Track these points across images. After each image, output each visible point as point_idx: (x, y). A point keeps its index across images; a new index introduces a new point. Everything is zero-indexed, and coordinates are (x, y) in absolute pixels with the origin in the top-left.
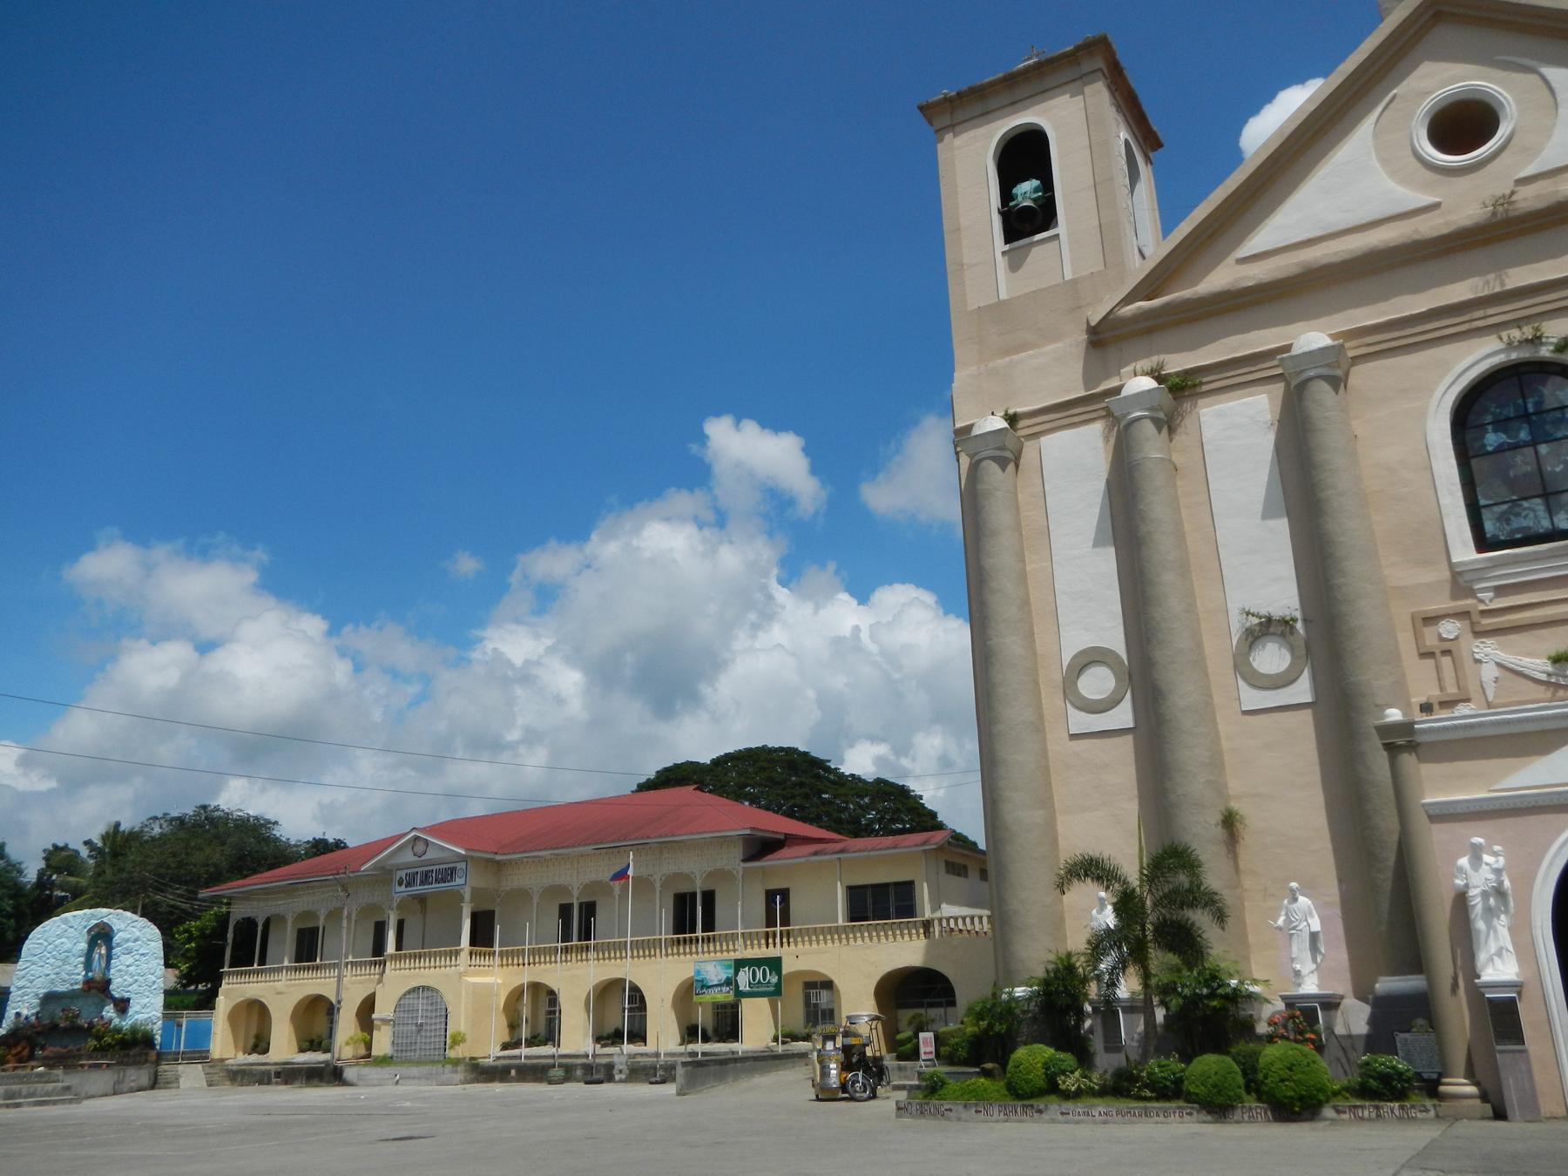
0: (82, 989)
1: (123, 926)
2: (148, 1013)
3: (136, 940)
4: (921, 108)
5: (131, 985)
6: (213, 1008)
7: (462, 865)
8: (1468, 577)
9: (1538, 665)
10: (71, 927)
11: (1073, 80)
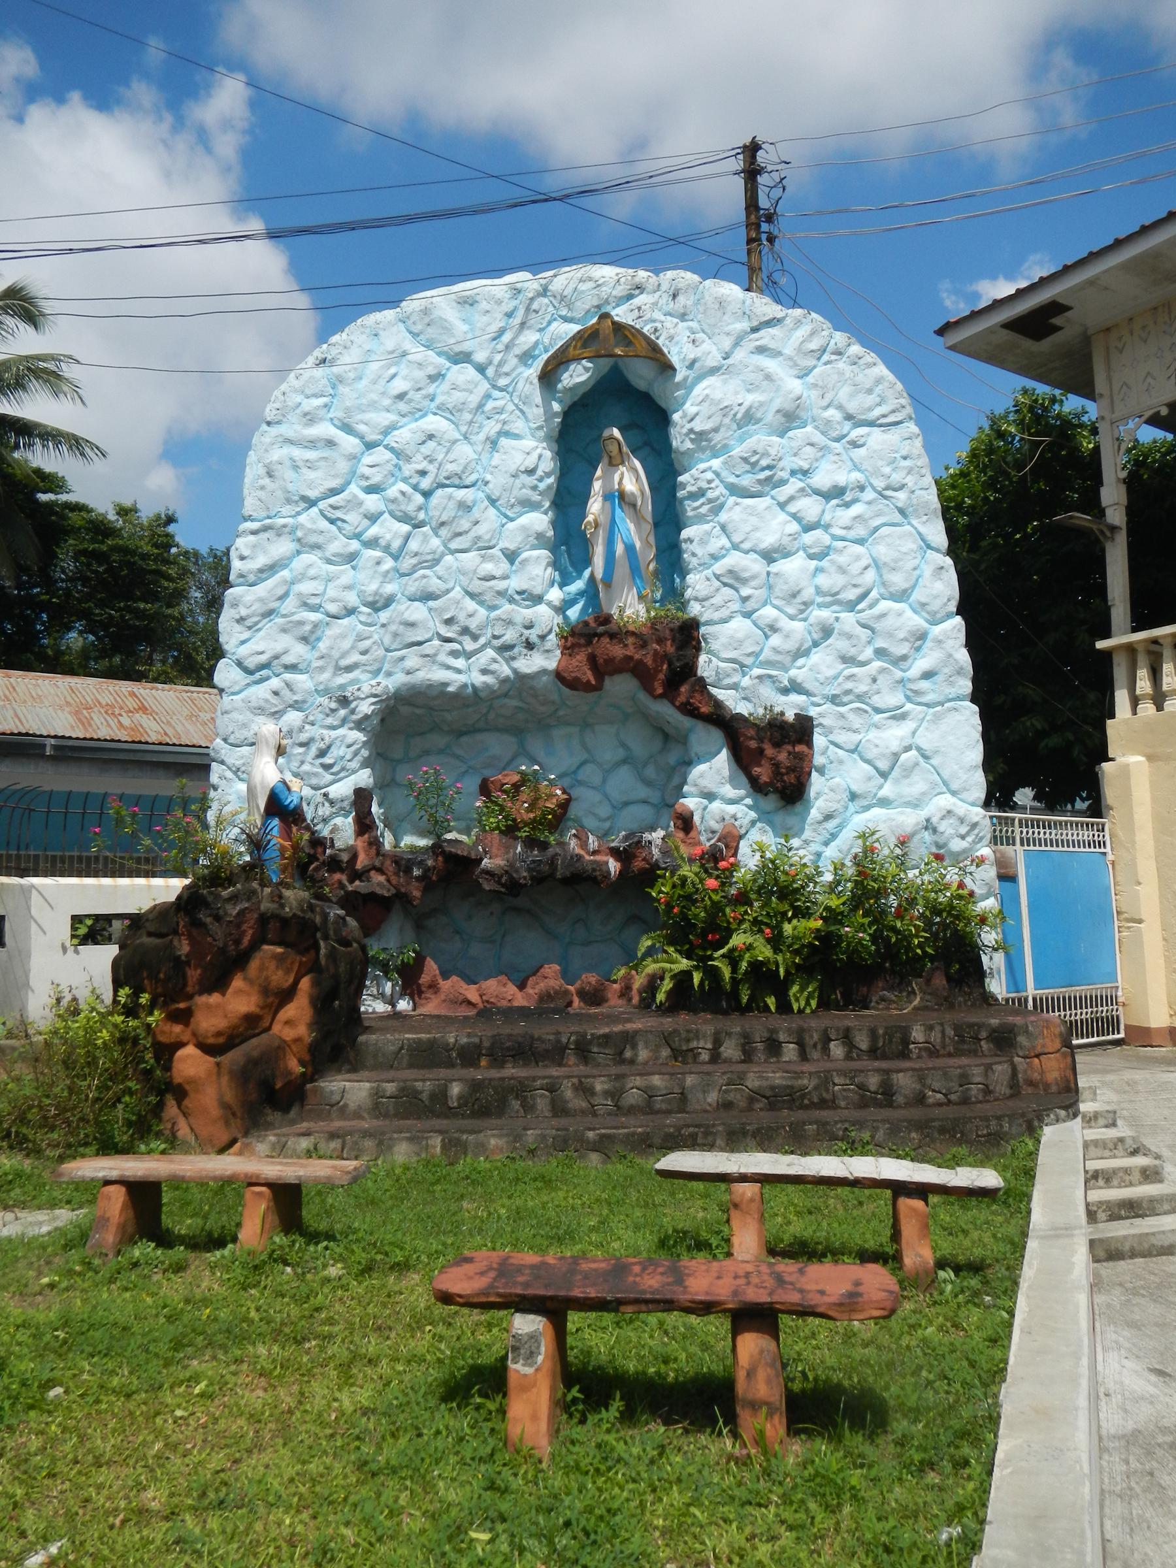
0: (558, 675)
1: (710, 351)
2: (915, 804)
3: (790, 418)
5: (801, 653)
6: (1097, 810)
10: (462, 358)
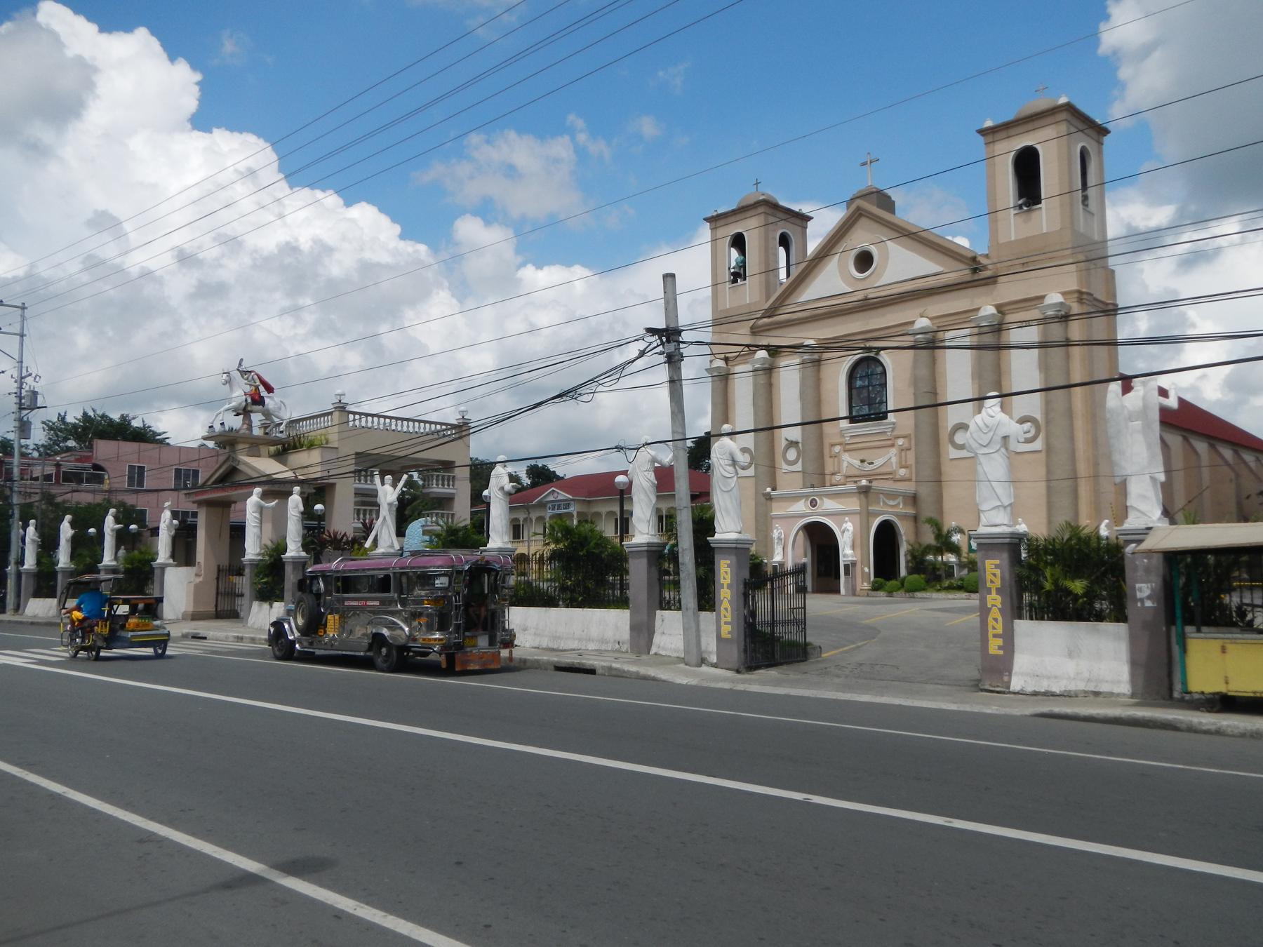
4: (704, 219)
7: (572, 502)
8: (843, 432)
9: (857, 463)
11: (755, 215)
